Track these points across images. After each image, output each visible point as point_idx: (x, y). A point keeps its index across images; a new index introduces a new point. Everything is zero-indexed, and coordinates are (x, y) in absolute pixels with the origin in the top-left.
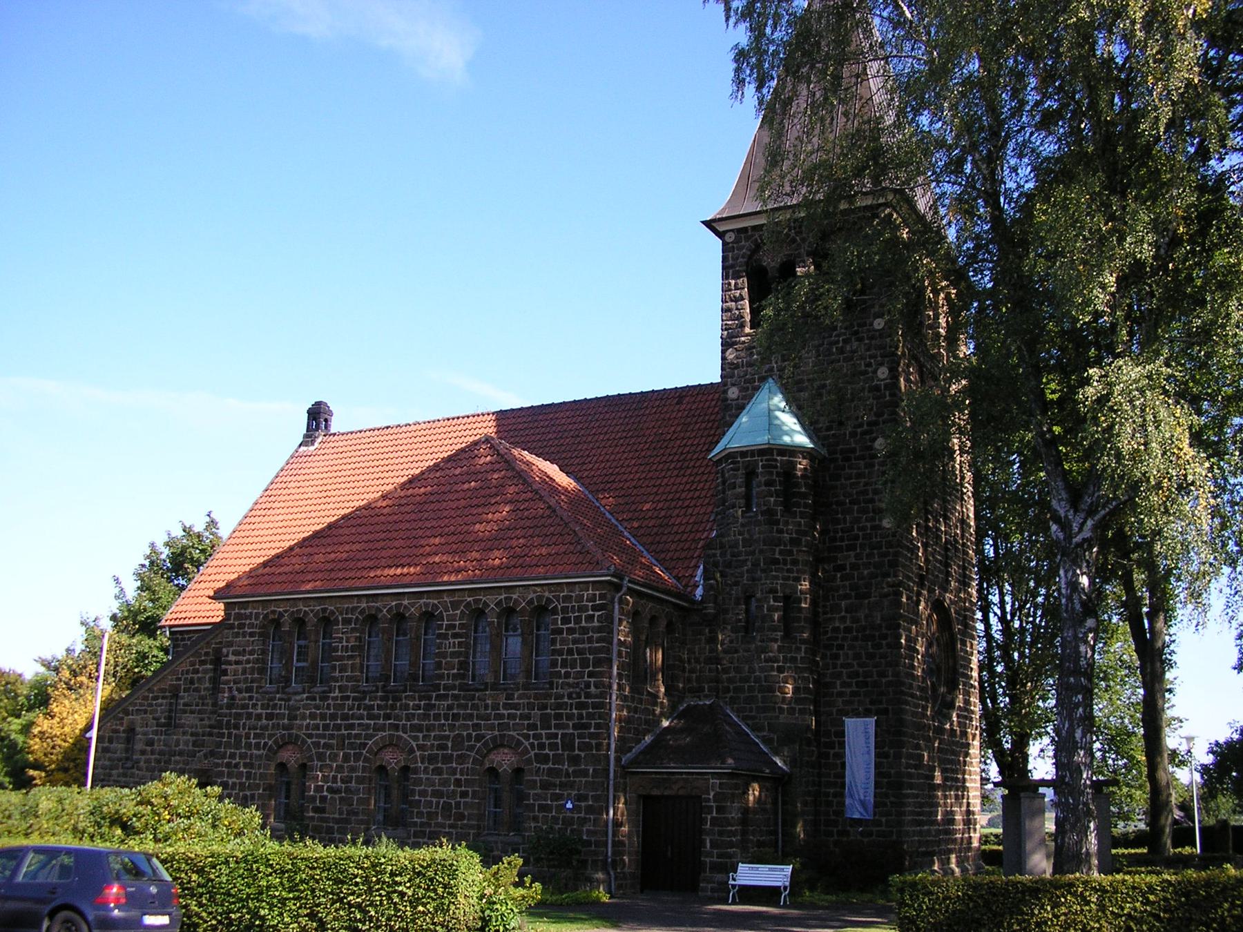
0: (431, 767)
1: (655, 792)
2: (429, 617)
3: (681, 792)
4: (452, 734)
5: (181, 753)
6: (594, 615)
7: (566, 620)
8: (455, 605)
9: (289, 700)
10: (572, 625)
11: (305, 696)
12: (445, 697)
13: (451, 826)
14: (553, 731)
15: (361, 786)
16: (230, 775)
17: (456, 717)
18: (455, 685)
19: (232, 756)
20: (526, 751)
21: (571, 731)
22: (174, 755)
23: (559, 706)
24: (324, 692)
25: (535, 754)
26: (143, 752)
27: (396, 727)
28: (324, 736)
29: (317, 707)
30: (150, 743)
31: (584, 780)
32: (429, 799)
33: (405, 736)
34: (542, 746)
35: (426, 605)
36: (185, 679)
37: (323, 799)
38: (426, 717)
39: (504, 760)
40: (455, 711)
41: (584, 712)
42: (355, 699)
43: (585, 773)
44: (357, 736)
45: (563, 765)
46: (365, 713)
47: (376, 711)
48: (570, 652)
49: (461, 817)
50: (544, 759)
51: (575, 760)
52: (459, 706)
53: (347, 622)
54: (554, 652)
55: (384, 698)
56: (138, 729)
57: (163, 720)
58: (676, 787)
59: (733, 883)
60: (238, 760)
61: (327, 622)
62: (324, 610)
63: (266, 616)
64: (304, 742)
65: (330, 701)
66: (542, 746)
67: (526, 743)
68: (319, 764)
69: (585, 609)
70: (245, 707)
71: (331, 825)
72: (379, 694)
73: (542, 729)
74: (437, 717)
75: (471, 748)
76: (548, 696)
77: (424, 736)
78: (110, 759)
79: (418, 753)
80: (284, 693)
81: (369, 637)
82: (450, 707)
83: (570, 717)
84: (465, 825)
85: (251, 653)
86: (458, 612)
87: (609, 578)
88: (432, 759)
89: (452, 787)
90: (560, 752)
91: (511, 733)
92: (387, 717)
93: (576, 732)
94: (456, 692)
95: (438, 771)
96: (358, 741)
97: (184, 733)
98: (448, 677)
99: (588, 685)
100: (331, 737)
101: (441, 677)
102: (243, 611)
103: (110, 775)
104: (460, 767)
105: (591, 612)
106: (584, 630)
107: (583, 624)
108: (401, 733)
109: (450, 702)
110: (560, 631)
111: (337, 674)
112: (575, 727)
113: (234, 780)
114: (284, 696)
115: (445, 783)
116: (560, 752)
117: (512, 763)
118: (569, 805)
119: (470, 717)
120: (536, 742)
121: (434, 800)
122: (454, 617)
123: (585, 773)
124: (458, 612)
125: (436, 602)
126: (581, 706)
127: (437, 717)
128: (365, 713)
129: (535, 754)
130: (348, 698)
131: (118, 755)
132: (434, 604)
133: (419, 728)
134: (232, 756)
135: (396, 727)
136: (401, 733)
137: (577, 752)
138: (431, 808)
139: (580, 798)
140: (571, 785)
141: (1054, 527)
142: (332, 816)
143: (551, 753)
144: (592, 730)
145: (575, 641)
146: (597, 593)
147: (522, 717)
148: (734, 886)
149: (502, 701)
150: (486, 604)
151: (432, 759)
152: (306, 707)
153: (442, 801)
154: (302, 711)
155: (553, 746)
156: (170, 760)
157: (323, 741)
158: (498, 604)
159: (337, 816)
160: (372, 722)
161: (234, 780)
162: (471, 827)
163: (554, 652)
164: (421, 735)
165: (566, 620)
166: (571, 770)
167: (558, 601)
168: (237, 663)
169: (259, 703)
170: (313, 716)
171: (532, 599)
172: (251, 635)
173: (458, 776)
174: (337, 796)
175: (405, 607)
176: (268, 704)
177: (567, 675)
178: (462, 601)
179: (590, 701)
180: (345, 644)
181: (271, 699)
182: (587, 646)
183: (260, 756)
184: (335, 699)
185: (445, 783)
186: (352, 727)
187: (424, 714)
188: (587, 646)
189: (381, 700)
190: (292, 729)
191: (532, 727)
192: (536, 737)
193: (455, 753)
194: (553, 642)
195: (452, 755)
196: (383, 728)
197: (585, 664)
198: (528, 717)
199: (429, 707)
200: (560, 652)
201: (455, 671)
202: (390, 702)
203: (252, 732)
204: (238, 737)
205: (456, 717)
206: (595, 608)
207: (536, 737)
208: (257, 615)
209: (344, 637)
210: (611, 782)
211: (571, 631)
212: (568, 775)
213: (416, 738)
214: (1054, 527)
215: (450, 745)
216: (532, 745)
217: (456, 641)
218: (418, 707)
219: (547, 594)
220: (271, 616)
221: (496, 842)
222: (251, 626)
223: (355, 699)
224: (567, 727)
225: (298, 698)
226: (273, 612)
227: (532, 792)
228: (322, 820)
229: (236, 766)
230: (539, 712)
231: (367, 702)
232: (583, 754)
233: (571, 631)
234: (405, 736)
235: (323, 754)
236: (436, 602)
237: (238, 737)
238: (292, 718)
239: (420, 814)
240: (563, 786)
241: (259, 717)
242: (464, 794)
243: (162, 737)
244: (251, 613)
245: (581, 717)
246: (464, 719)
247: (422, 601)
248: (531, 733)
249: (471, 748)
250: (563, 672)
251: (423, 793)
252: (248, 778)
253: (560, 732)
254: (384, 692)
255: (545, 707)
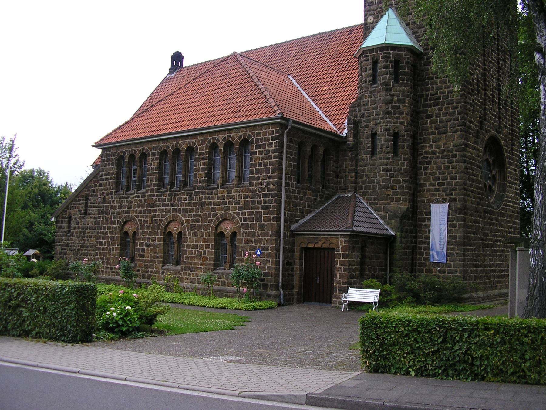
0: (192, 232)
1: (311, 246)
2: (190, 150)
3: (324, 246)
4: (202, 214)
5: (90, 228)
6: (272, 143)
7: (258, 147)
8: (203, 142)
9: (128, 198)
10: (261, 149)
11: (135, 195)
12: (198, 193)
13: (201, 264)
14: (251, 210)
15: (160, 243)
16: (104, 239)
17: (204, 204)
18: (203, 186)
19: (104, 228)
20: (237, 222)
21: (261, 210)
22: (87, 229)
23: (254, 196)
24: (143, 193)
25: (242, 223)
26: (75, 228)
27: (175, 211)
28: (143, 217)
29: (140, 201)
30: (78, 223)
31: (266, 238)
32: (191, 249)
33: (180, 215)
34: (245, 219)
35: (190, 142)
36: (92, 190)
37: (143, 249)
38: (189, 204)
39: (227, 228)
40: (203, 201)
41: (267, 199)
42: (157, 196)
43: (267, 235)
44: (158, 216)
45: (256, 230)
46: (162, 203)
47: (166, 202)
48: (260, 165)
49: (206, 259)
50: (246, 226)
51: (262, 227)
52: (205, 198)
53: (153, 154)
54: (251, 165)
55: (170, 195)
56: (73, 216)
57: (82, 211)
58: (320, 243)
59: (345, 299)
60: (107, 230)
61: (144, 156)
62: (143, 149)
63: (118, 154)
64: (135, 219)
65: (146, 198)
66: (245, 219)
67: (238, 218)
68: (142, 231)
69: (266, 140)
70: (109, 202)
71: (147, 263)
72: (168, 193)
73: (246, 209)
74: (195, 204)
75: (211, 221)
76: (249, 191)
77: (189, 215)
78: (62, 232)
79: (186, 224)
80: (126, 194)
81: (165, 162)
82: (201, 199)
83: (260, 202)
84: (208, 264)
85: (112, 174)
86: (205, 145)
87: (279, 120)
88: (193, 228)
89: (202, 243)
90: (255, 222)
91: (230, 212)
92: (172, 205)
93: (262, 211)
94: (204, 190)
95: (195, 234)
96: (158, 219)
97: (91, 218)
98: (200, 182)
99: (269, 184)
100: (147, 216)
101: (197, 182)
102: (108, 152)
103: (62, 240)
104: (205, 231)
105: (271, 141)
106: (268, 152)
107: (267, 148)
108: (178, 214)
109: (201, 196)
110: (255, 153)
111: (149, 183)
112: (262, 208)
113: (105, 240)
114: (126, 196)
115: (198, 241)
116: (255, 222)
117: (231, 229)
118: (259, 253)
119: (210, 204)
120: (242, 217)
121: (193, 250)
122: (202, 149)
123: (267, 235)
124: (205, 145)
125: (194, 140)
126: (266, 195)
127: (195, 204)
128: (162, 203)
129: (242, 223)
130: (154, 195)
131: (65, 230)
132: (193, 142)
133: (186, 211)
134: (104, 228)
135: (175, 211)
136: (178, 214)
137: (263, 222)
138: (192, 254)
139: (265, 249)
140: (260, 241)
141: (537, 56)
142: (147, 259)
143: (250, 223)
144: (271, 210)
145: (262, 159)
146: (274, 130)
147: (236, 203)
148: (345, 302)
149: (226, 194)
150: (218, 140)
151: (193, 228)
152: (135, 201)
153: (197, 250)
154: (134, 203)
155: (251, 219)
156: (86, 231)
157: (143, 219)
158: (225, 138)
159: (149, 259)
160: (165, 208)
161: (105, 240)
162: (210, 264)
163: (251, 165)
164: (187, 214)
165: (258, 147)
166: (260, 233)
167: (254, 136)
168: (106, 179)
169: (115, 200)
170: (139, 206)
171: (241, 135)
172: (112, 164)
173: (205, 237)
174: (149, 248)
175: (180, 144)
176: (119, 200)
177: (258, 178)
178: (207, 139)
179: (270, 193)
180: (152, 166)
181: (121, 198)
182: (268, 161)
183: (115, 228)
184: (148, 196)
185: (198, 241)
186: (155, 211)
187: (189, 203)
188: (268, 161)
189: (169, 196)
190: (130, 213)
191: (241, 208)
192: (243, 214)
193: (203, 224)
194: (251, 159)
195: (202, 225)
196: (169, 211)
197: (267, 171)
198: (238, 203)
199: (191, 199)
200: (255, 165)
201: (203, 178)
202: (173, 197)
203: (113, 215)
204: (107, 218)
205: (204, 204)
206: (273, 139)
207: (243, 214)
208: (115, 153)
209: (152, 163)
210: (282, 239)
211: (261, 153)
212: (258, 235)
213: (185, 216)
214: (537, 56)
215: (201, 219)
216: (240, 218)
217: (204, 161)
218: (186, 199)
219: (248, 132)
220: (120, 154)
221: (223, 274)
222: (113, 160)
223: (157, 196)
224: (258, 208)
225: (132, 196)
226: (121, 152)
227: (240, 245)
228: (143, 261)
229: (106, 233)
230: (244, 200)
231: (162, 197)
232: (266, 223)
233: (261, 153)
234: (180, 215)
235: (143, 226)
236: (194, 140)
237: (107, 218)
238: (130, 207)
239: (187, 258)
240: (256, 242)
241: (115, 207)
242: (207, 247)
243: (82, 220)
244: (112, 153)
245: (265, 202)
246: (208, 205)
247: (188, 141)
248: (240, 212)
249: (211, 221)
250: (256, 176)
251: (188, 246)
252: (111, 239)
253: (254, 211)
254: (170, 191)
255: (247, 197)
